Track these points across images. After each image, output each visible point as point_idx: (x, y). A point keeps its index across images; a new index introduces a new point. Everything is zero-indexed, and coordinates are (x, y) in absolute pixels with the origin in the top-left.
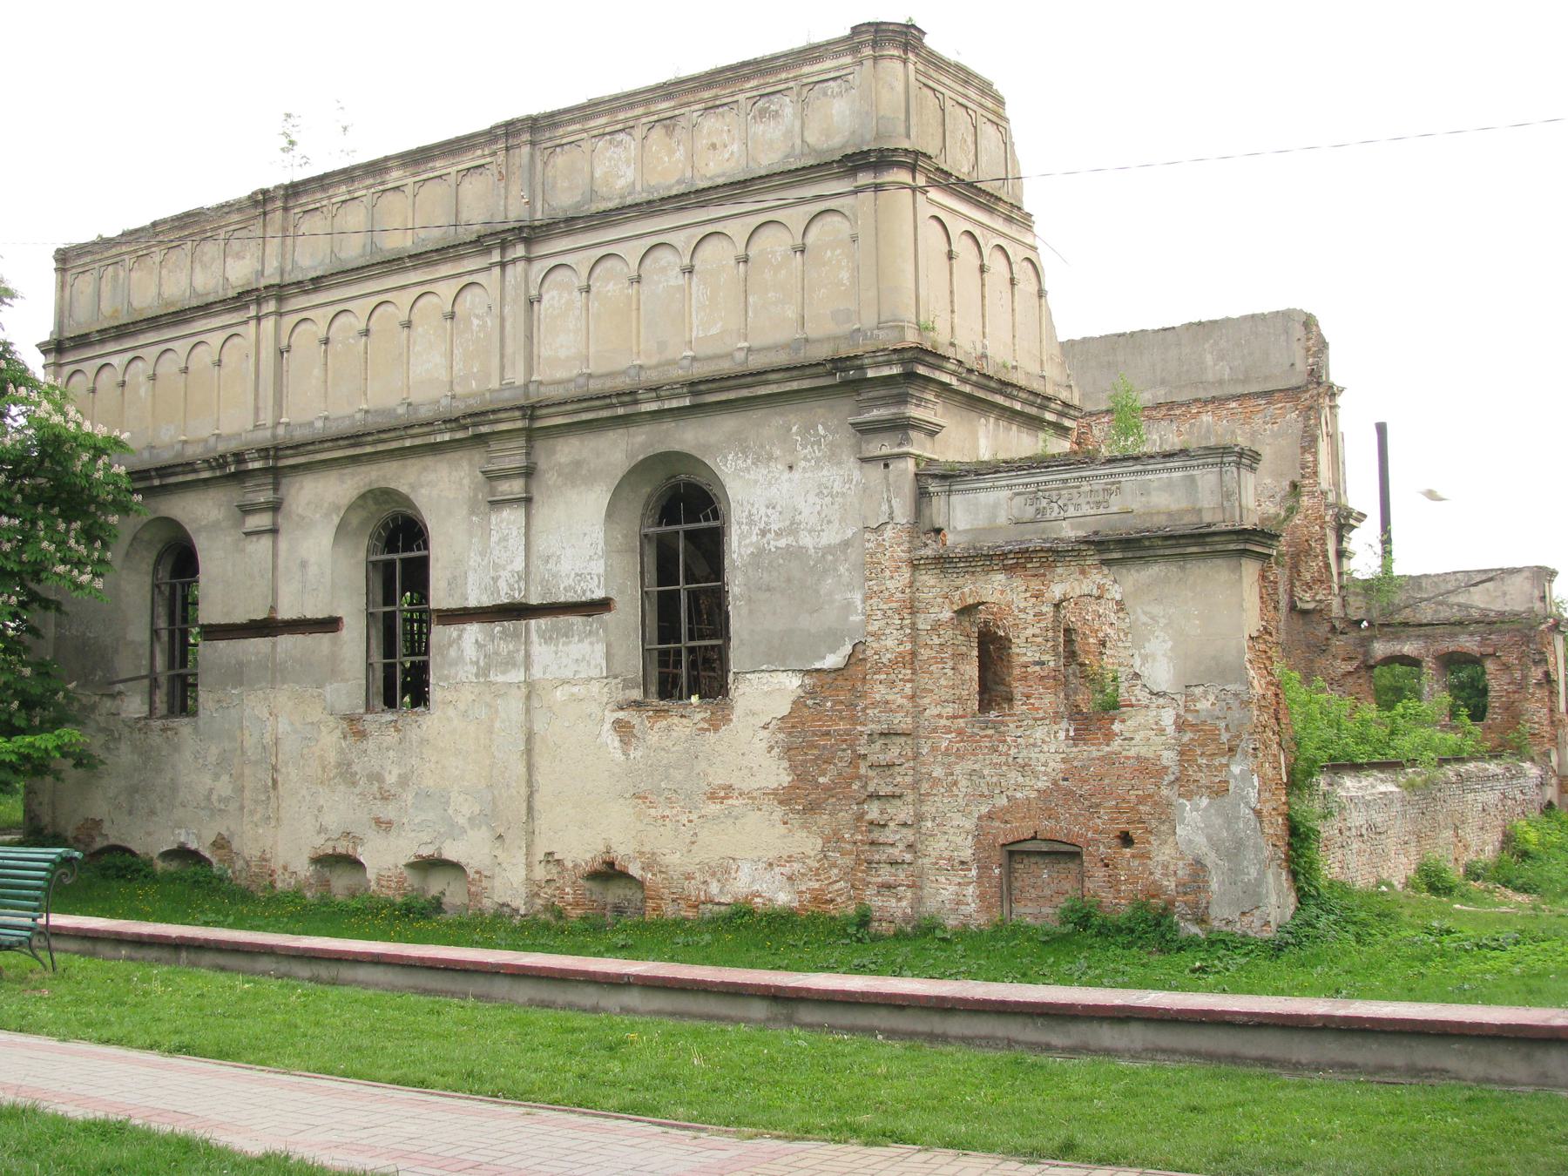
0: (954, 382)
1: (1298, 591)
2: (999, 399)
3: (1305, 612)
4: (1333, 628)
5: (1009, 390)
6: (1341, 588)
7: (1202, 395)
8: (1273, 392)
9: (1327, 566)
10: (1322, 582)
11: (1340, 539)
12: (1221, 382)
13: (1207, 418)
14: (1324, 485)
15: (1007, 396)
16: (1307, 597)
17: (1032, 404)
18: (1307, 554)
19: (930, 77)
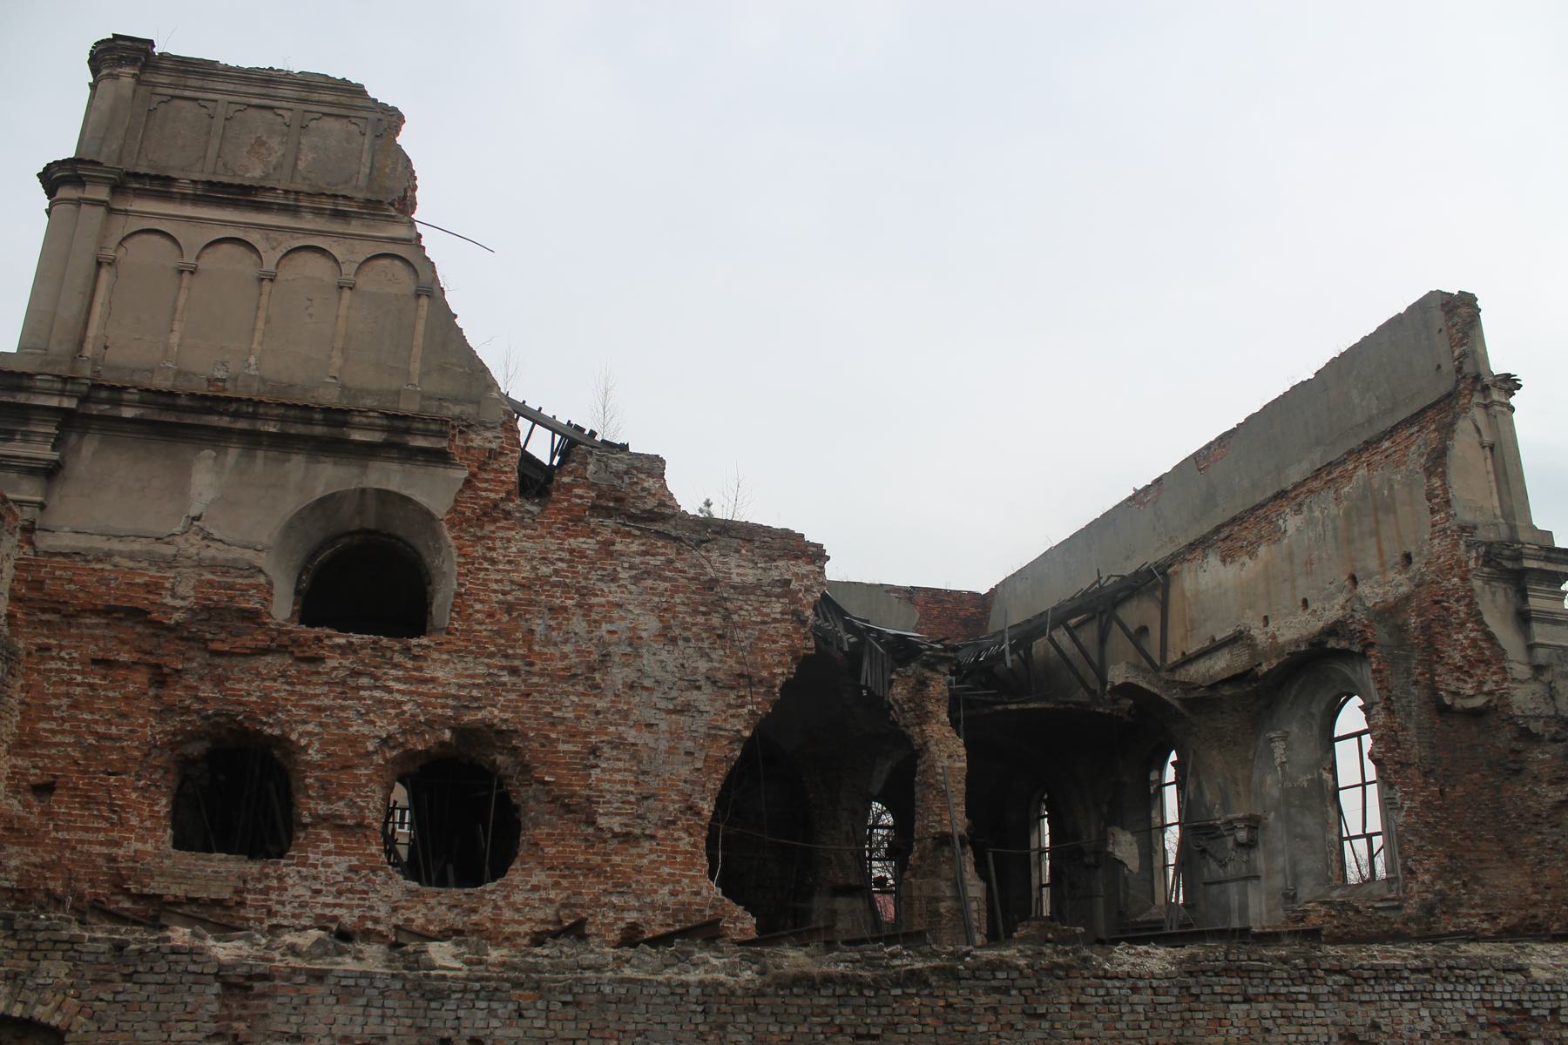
0: (69, 403)
1: (1447, 681)
2: (214, 420)
3: (1476, 714)
4: (1526, 734)
5: (234, 406)
6: (1538, 669)
7: (1354, 443)
8: (1424, 411)
9: (1490, 637)
10: (1488, 663)
11: (1523, 595)
12: (1370, 420)
13: (1362, 472)
14: (1468, 517)
15: (236, 415)
16: (1468, 689)
17: (310, 422)
18: (1446, 624)
19: (186, 87)
